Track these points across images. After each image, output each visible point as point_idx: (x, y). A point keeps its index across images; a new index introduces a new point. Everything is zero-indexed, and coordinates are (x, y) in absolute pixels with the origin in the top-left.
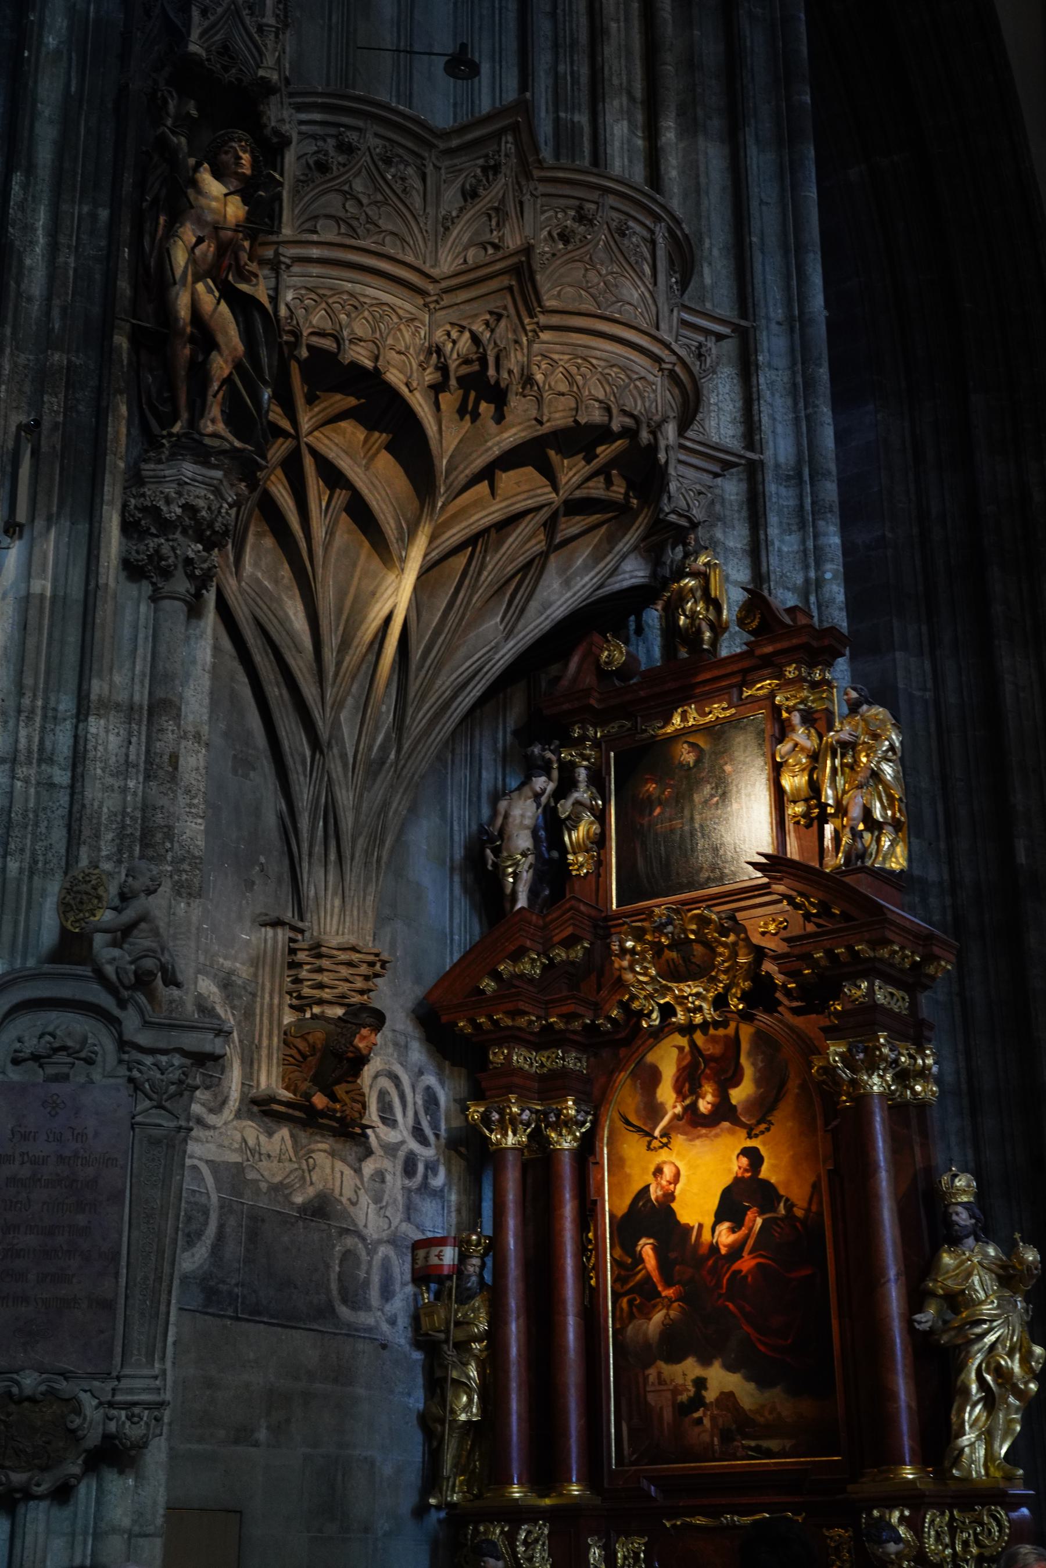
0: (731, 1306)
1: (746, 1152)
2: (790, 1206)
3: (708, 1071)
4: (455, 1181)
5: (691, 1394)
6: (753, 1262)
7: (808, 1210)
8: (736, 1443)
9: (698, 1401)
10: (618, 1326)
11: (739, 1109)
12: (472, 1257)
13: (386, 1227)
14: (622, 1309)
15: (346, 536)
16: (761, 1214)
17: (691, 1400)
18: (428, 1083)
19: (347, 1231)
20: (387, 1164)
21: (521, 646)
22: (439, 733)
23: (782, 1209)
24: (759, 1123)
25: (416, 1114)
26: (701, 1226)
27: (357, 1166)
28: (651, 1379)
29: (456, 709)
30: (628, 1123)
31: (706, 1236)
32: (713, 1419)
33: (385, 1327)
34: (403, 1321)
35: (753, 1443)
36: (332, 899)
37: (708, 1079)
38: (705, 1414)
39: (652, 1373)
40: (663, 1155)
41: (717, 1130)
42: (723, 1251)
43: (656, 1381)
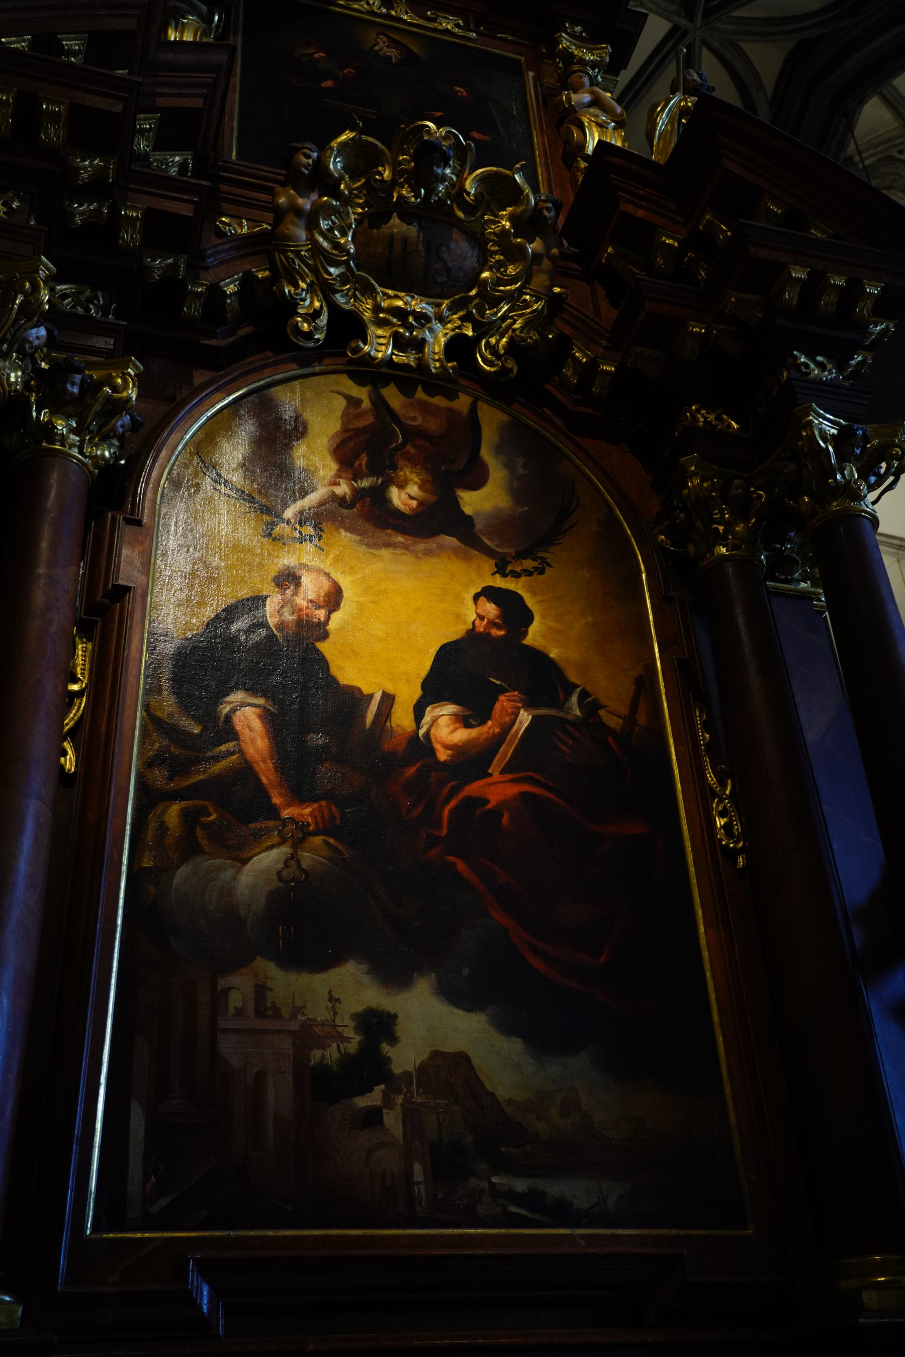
0: (461, 866)
1: (489, 593)
2: (591, 706)
6: (513, 790)
7: (630, 719)
8: (473, 1182)
10: (147, 863)
11: (479, 526)
17: (349, 1063)
24: (520, 556)
26: (388, 700)
28: (235, 1000)
32: (410, 1114)
35: (520, 1185)
37: (413, 462)
38: (388, 1102)
41: (432, 544)
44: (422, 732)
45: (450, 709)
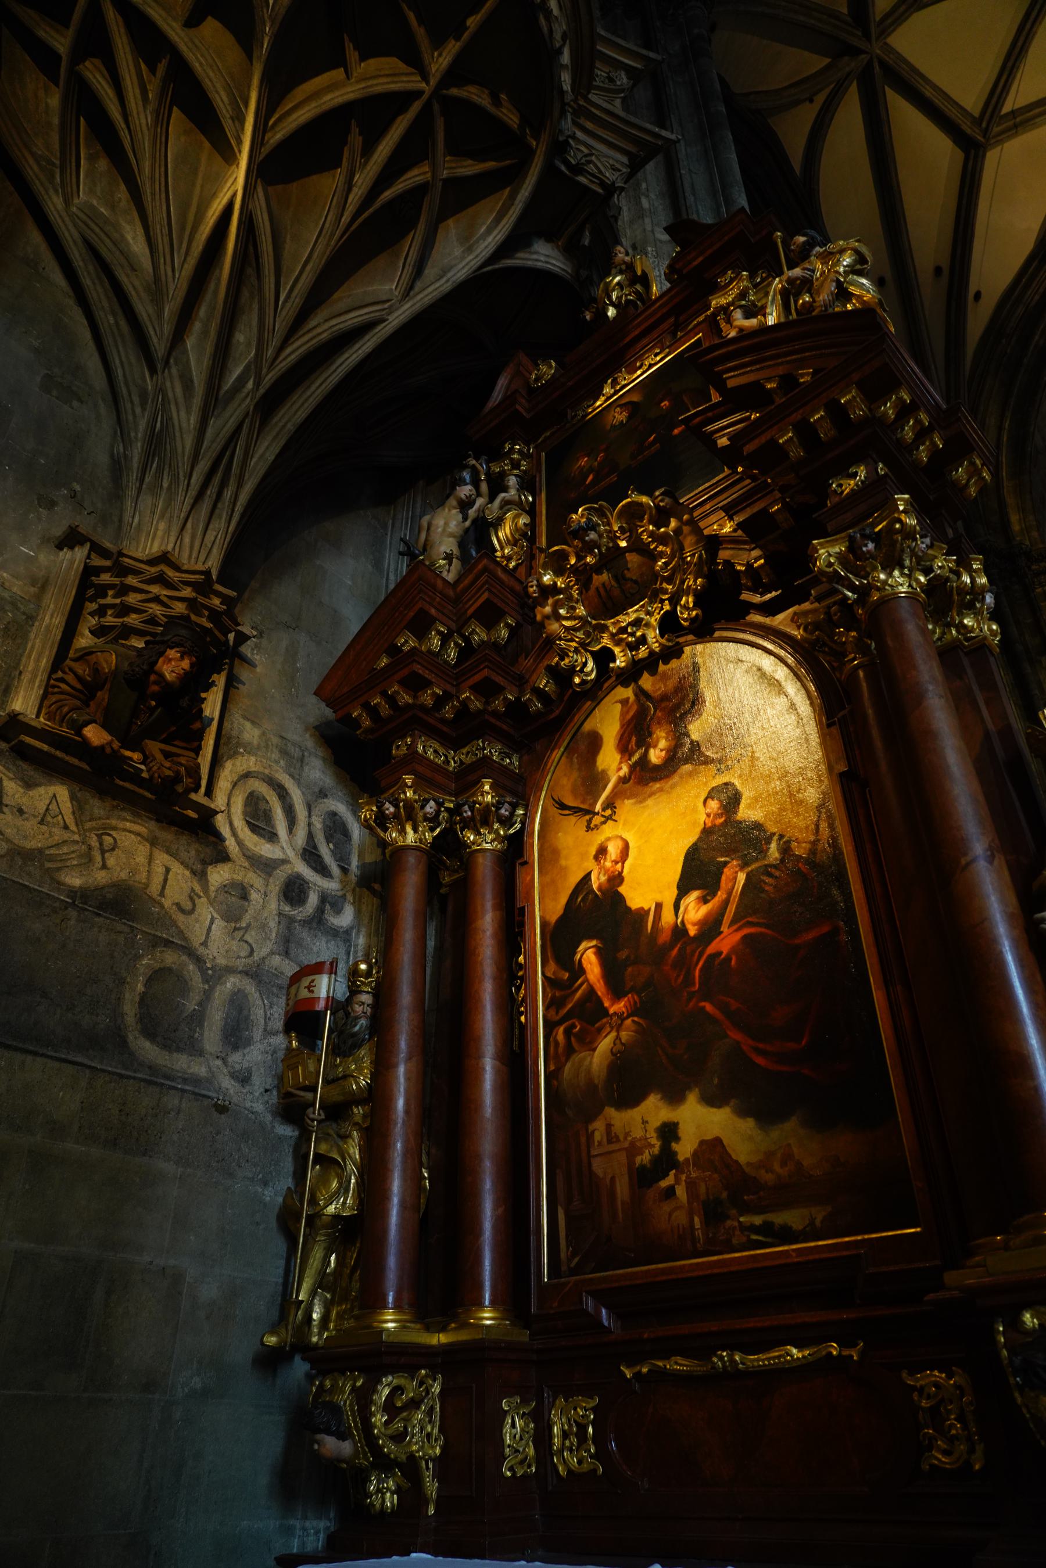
0: (708, 1007)
3: (659, 714)
4: (366, 921)
5: (656, 1150)
6: (738, 936)
8: (729, 1223)
9: (666, 1161)
12: (361, 992)
13: (243, 954)
14: (557, 1043)
15: (183, 139)
16: (742, 868)
17: (656, 1160)
18: (333, 808)
19: (168, 943)
20: (254, 879)
21: (418, 307)
22: (321, 385)
23: (774, 851)
25: (310, 836)
26: (659, 906)
27: (198, 867)
28: (597, 1136)
29: (341, 365)
30: (562, 806)
31: (668, 917)
32: (691, 1185)
33: (227, 1083)
34: (260, 1081)
35: (758, 1220)
36: (157, 522)
38: (677, 1180)
39: (598, 1127)
40: (608, 830)
42: (692, 931)
43: (605, 1140)
44: (679, 921)
45: (694, 895)
